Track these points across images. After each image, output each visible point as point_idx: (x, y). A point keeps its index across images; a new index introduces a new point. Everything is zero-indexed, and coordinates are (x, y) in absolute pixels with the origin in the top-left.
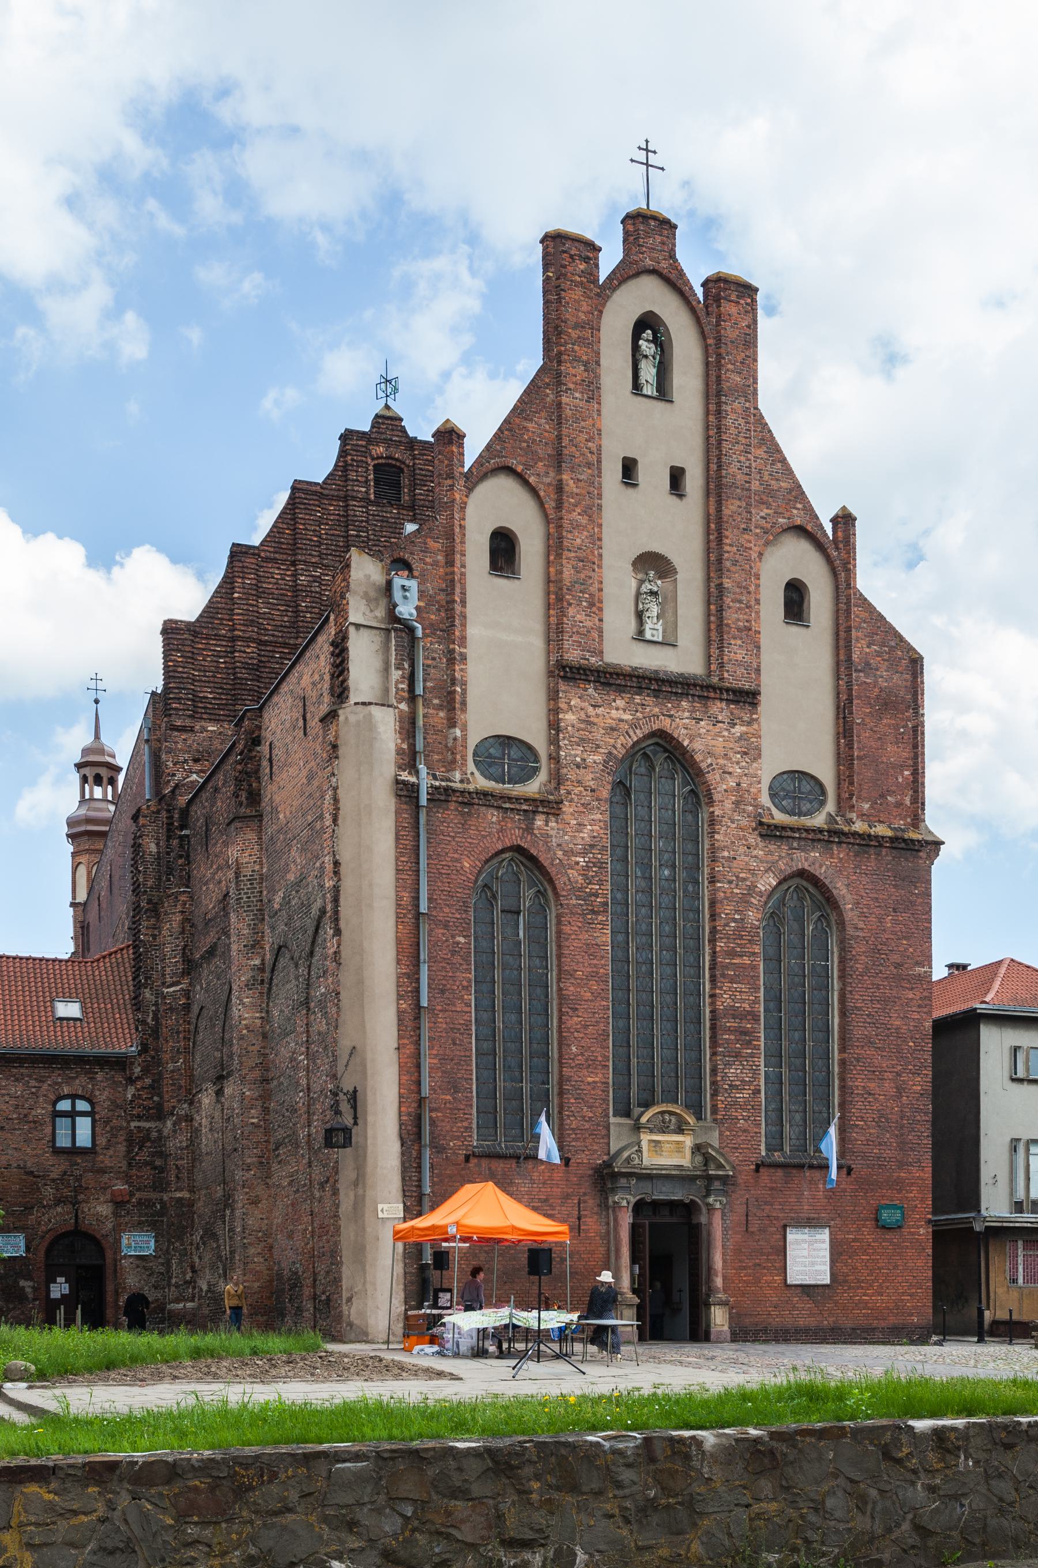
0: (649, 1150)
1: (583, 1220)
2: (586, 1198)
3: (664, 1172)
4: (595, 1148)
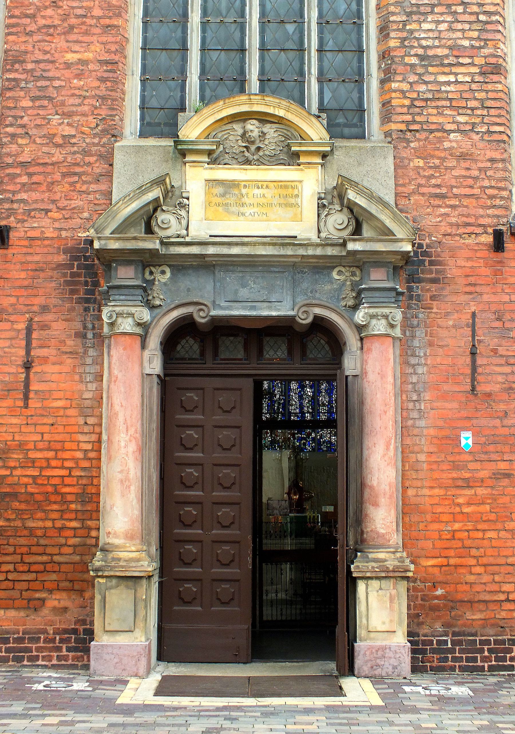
0: (208, 204)
1: (36, 368)
2: (49, 317)
3: (235, 250)
4: (77, 203)
